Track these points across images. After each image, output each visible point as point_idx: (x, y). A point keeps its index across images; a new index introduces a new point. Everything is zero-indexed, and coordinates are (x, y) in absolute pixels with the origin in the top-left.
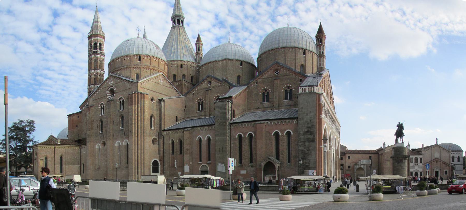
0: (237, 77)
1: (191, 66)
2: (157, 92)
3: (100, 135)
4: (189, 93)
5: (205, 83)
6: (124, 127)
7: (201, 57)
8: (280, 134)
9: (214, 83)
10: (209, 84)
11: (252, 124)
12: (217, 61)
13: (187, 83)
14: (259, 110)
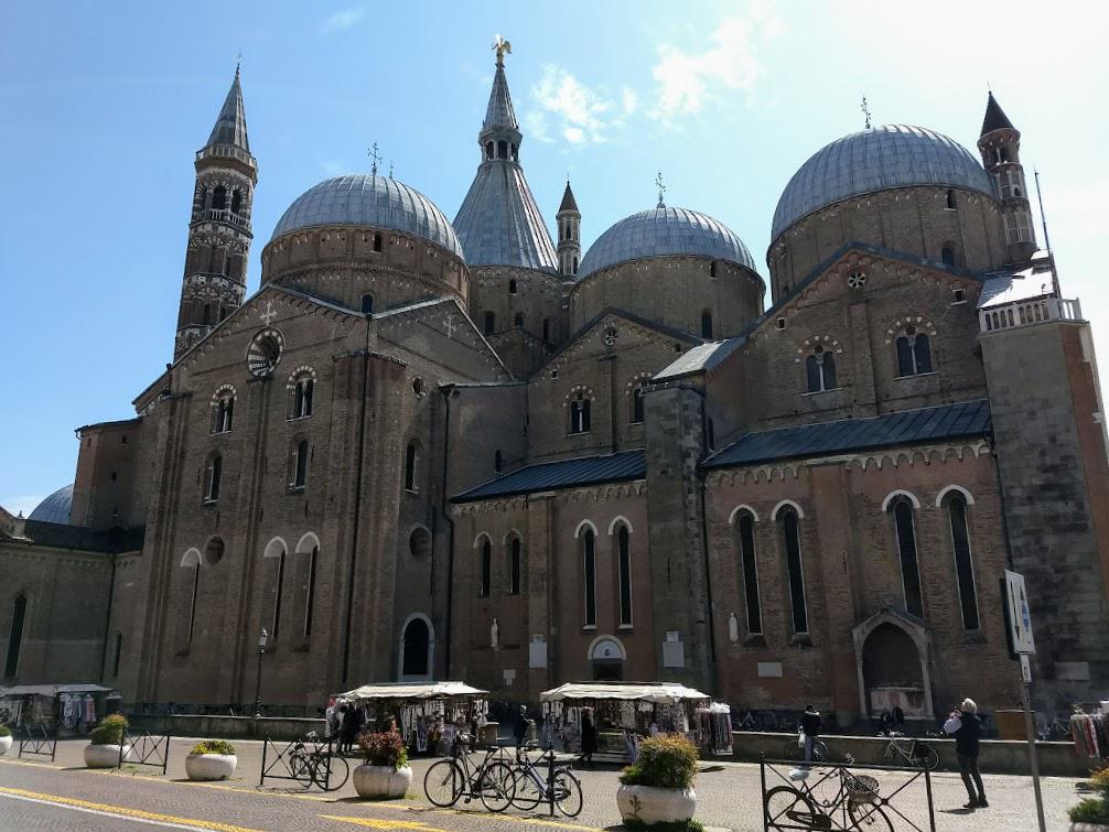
3: (206, 512)
6: (306, 480)
8: (917, 504)
9: (629, 334)
12: (632, 261)
13: (533, 341)
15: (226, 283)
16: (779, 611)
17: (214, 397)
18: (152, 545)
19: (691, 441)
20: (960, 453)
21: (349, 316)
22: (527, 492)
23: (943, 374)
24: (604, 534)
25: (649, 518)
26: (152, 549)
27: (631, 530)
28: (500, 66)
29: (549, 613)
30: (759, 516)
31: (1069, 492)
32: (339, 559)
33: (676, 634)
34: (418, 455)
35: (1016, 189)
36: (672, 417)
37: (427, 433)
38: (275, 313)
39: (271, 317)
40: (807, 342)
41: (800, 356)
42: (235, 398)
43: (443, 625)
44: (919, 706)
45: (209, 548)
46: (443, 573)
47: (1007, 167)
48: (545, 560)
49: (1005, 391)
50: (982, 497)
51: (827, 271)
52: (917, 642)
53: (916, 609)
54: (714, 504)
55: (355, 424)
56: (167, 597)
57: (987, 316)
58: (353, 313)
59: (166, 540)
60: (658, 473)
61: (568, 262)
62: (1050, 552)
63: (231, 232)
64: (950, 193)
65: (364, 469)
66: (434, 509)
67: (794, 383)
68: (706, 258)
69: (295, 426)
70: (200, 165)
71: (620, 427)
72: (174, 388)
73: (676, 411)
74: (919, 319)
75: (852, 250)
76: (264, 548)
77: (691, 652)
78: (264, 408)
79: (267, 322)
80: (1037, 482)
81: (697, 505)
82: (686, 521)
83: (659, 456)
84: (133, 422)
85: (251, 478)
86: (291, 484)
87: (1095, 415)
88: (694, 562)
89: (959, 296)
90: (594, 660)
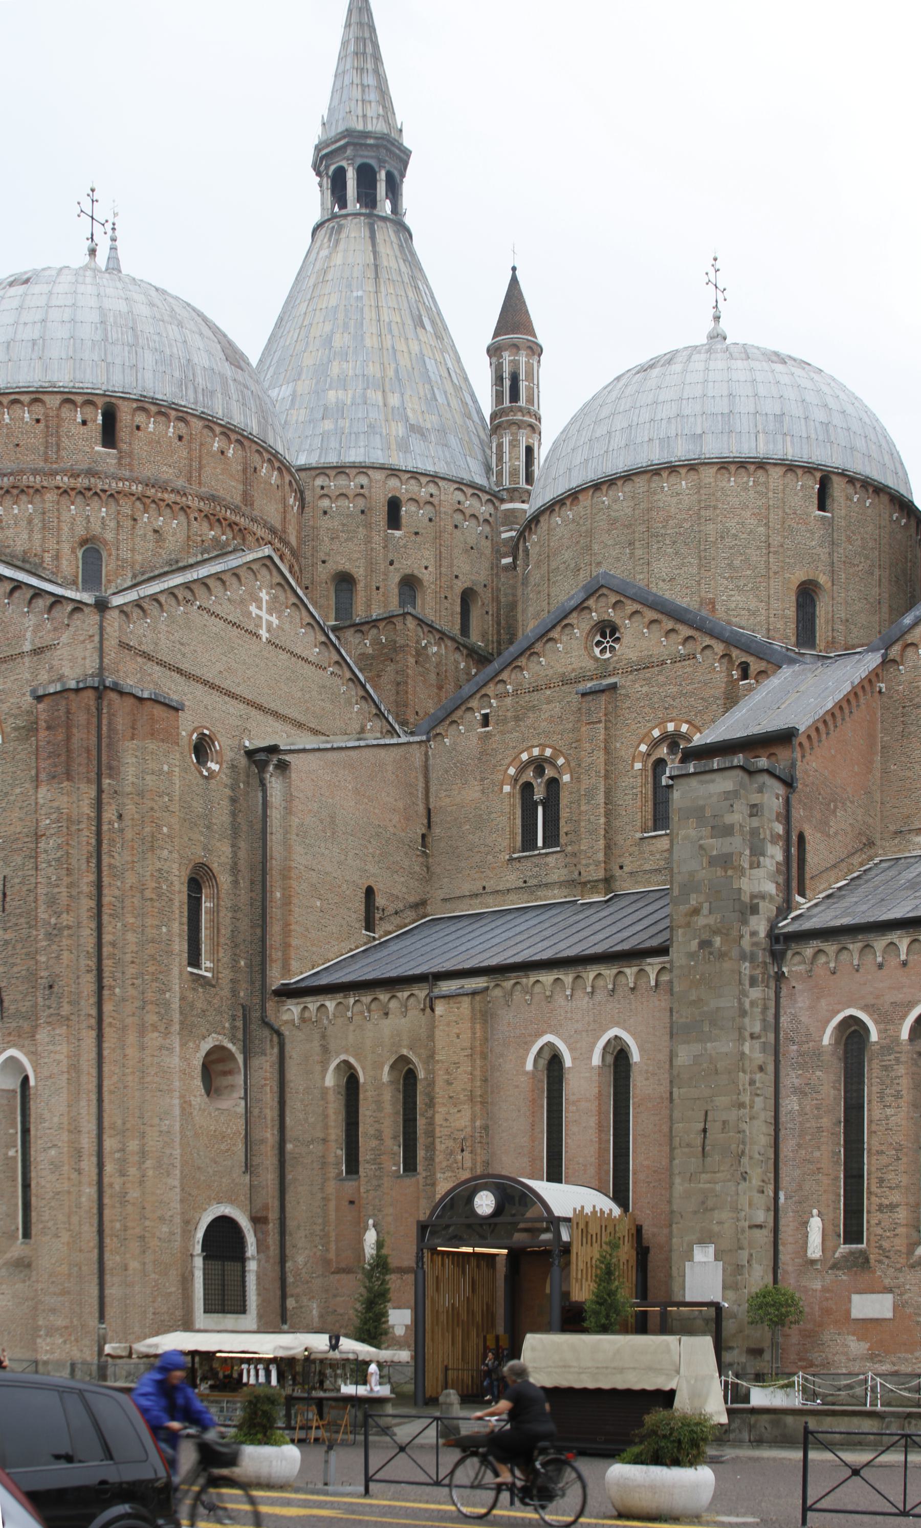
0: (794, 598)
10: (599, 643)
16: (897, 1206)
27: (636, 1056)
30: (880, 1032)
34: (211, 898)
37: (225, 849)
60: (694, 944)
65: (107, 928)
71: (619, 839)
81: (765, 1009)
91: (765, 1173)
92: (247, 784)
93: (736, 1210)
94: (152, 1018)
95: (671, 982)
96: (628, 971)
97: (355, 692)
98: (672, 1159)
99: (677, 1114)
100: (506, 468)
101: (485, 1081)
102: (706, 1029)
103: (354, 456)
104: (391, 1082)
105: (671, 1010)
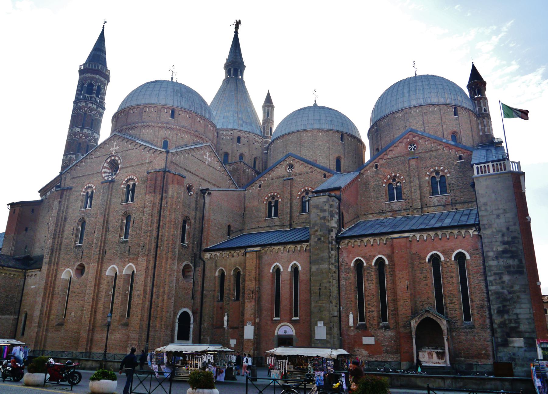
1: (254, 141)
2: (198, 176)
4: (253, 184)
5: (282, 167)
6: (129, 236)
7: (271, 129)
8: (443, 259)
9: (299, 168)
10: (288, 169)
11: (383, 240)
13: (248, 169)
14: (384, 215)
15: (90, 132)
17: (83, 190)
18: (47, 266)
19: (333, 224)
20: (463, 233)
21: (156, 150)
22: (246, 247)
23: (452, 195)
24: (286, 271)
25: (310, 263)
26: (47, 268)
27: (300, 269)
28: (236, 33)
29: (255, 312)
30: (366, 263)
31: (515, 254)
32: (146, 277)
33: (322, 323)
35: (485, 109)
36: (325, 211)
37: (194, 214)
38: (117, 148)
39: (115, 150)
40: (389, 176)
41: (385, 183)
42: (94, 191)
43: (198, 315)
44: (442, 359)
45: (77, 269)
46: (199, 289)
47: (480, 98)
48: (254, 284)
49: (485, 204)
50: (474, 256)
51: (398, 142)
52: (442, 327)
53: (440, 309)
54: (344, 256)
55: (157, 208)
56: (53, 294)
57: (477, 168)
58: (159, 149)
59: (54, 264)
60: (316, 239)
61: (268, 129)
62: (506, 283)
63: (95, 106)
64: (455, 108)
65: (160, 232)
66: (195, 254)
67: (382, 196)
68: (339, 132)
69: (125, 207)
70: (81, 72)
72: (62, 185)
73: (326, 208)
74: (442, 168)
75: (410, 133)
76: (106, 271)
77: (329, 332)
78: (109, 197)
79: (113, 152)
80: (500, 249)
81: (335, 256)
82: (329, 264)
83: (317, 231)
84: (38, 201)
85: (101, 233)
86: (122, 238)
87: (527, 217)
88: (333, 286)
89: (460, 158)
90: (278, 336)
91: (337, 301)
92: (200, 198)
93: (329, 311)
94: (170, 255)
95: (310, 250)
96: (298, 246)
97: (228, 178)
98: (311, 297)
99: (312, 284)
100: (265, 132)
101: (259, 275)
102: (320, 261)
103: (230, 127)
104: (233, 275)
105: (310, 257)
